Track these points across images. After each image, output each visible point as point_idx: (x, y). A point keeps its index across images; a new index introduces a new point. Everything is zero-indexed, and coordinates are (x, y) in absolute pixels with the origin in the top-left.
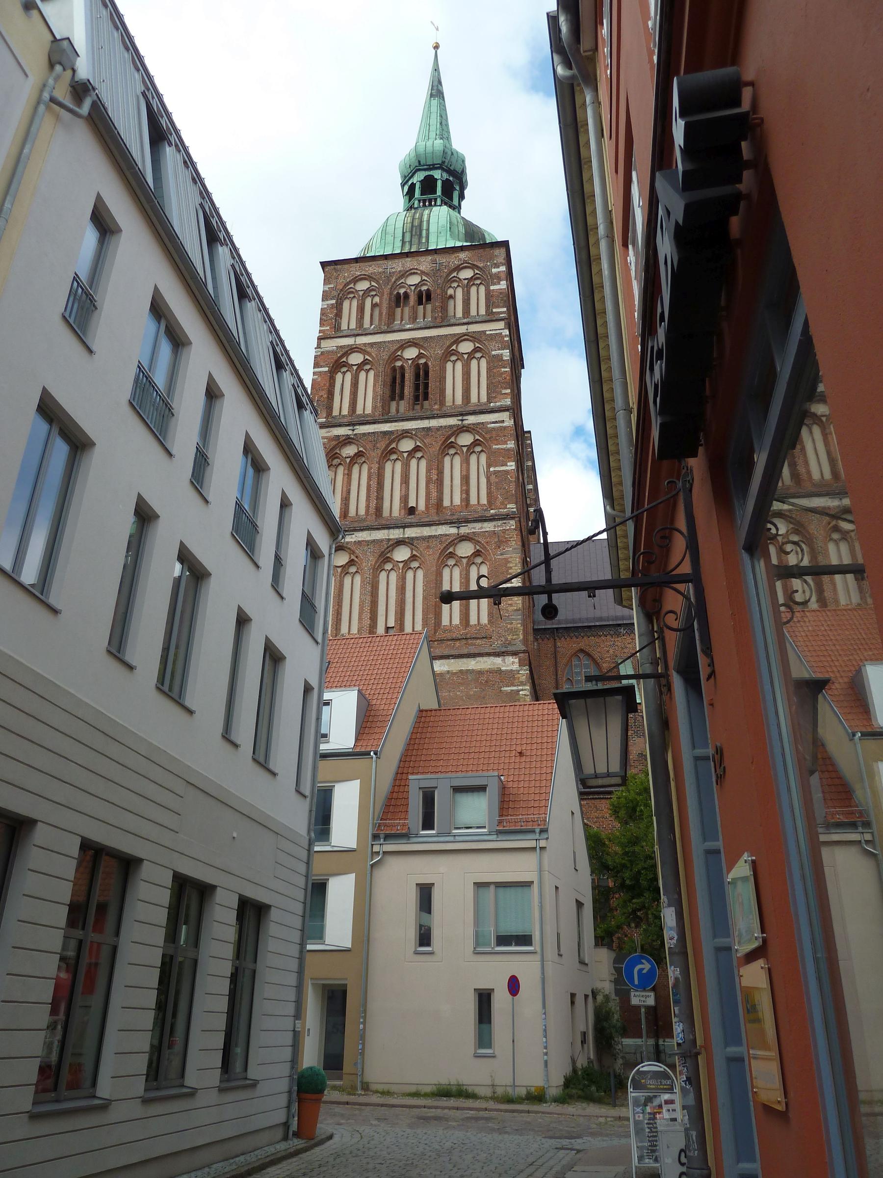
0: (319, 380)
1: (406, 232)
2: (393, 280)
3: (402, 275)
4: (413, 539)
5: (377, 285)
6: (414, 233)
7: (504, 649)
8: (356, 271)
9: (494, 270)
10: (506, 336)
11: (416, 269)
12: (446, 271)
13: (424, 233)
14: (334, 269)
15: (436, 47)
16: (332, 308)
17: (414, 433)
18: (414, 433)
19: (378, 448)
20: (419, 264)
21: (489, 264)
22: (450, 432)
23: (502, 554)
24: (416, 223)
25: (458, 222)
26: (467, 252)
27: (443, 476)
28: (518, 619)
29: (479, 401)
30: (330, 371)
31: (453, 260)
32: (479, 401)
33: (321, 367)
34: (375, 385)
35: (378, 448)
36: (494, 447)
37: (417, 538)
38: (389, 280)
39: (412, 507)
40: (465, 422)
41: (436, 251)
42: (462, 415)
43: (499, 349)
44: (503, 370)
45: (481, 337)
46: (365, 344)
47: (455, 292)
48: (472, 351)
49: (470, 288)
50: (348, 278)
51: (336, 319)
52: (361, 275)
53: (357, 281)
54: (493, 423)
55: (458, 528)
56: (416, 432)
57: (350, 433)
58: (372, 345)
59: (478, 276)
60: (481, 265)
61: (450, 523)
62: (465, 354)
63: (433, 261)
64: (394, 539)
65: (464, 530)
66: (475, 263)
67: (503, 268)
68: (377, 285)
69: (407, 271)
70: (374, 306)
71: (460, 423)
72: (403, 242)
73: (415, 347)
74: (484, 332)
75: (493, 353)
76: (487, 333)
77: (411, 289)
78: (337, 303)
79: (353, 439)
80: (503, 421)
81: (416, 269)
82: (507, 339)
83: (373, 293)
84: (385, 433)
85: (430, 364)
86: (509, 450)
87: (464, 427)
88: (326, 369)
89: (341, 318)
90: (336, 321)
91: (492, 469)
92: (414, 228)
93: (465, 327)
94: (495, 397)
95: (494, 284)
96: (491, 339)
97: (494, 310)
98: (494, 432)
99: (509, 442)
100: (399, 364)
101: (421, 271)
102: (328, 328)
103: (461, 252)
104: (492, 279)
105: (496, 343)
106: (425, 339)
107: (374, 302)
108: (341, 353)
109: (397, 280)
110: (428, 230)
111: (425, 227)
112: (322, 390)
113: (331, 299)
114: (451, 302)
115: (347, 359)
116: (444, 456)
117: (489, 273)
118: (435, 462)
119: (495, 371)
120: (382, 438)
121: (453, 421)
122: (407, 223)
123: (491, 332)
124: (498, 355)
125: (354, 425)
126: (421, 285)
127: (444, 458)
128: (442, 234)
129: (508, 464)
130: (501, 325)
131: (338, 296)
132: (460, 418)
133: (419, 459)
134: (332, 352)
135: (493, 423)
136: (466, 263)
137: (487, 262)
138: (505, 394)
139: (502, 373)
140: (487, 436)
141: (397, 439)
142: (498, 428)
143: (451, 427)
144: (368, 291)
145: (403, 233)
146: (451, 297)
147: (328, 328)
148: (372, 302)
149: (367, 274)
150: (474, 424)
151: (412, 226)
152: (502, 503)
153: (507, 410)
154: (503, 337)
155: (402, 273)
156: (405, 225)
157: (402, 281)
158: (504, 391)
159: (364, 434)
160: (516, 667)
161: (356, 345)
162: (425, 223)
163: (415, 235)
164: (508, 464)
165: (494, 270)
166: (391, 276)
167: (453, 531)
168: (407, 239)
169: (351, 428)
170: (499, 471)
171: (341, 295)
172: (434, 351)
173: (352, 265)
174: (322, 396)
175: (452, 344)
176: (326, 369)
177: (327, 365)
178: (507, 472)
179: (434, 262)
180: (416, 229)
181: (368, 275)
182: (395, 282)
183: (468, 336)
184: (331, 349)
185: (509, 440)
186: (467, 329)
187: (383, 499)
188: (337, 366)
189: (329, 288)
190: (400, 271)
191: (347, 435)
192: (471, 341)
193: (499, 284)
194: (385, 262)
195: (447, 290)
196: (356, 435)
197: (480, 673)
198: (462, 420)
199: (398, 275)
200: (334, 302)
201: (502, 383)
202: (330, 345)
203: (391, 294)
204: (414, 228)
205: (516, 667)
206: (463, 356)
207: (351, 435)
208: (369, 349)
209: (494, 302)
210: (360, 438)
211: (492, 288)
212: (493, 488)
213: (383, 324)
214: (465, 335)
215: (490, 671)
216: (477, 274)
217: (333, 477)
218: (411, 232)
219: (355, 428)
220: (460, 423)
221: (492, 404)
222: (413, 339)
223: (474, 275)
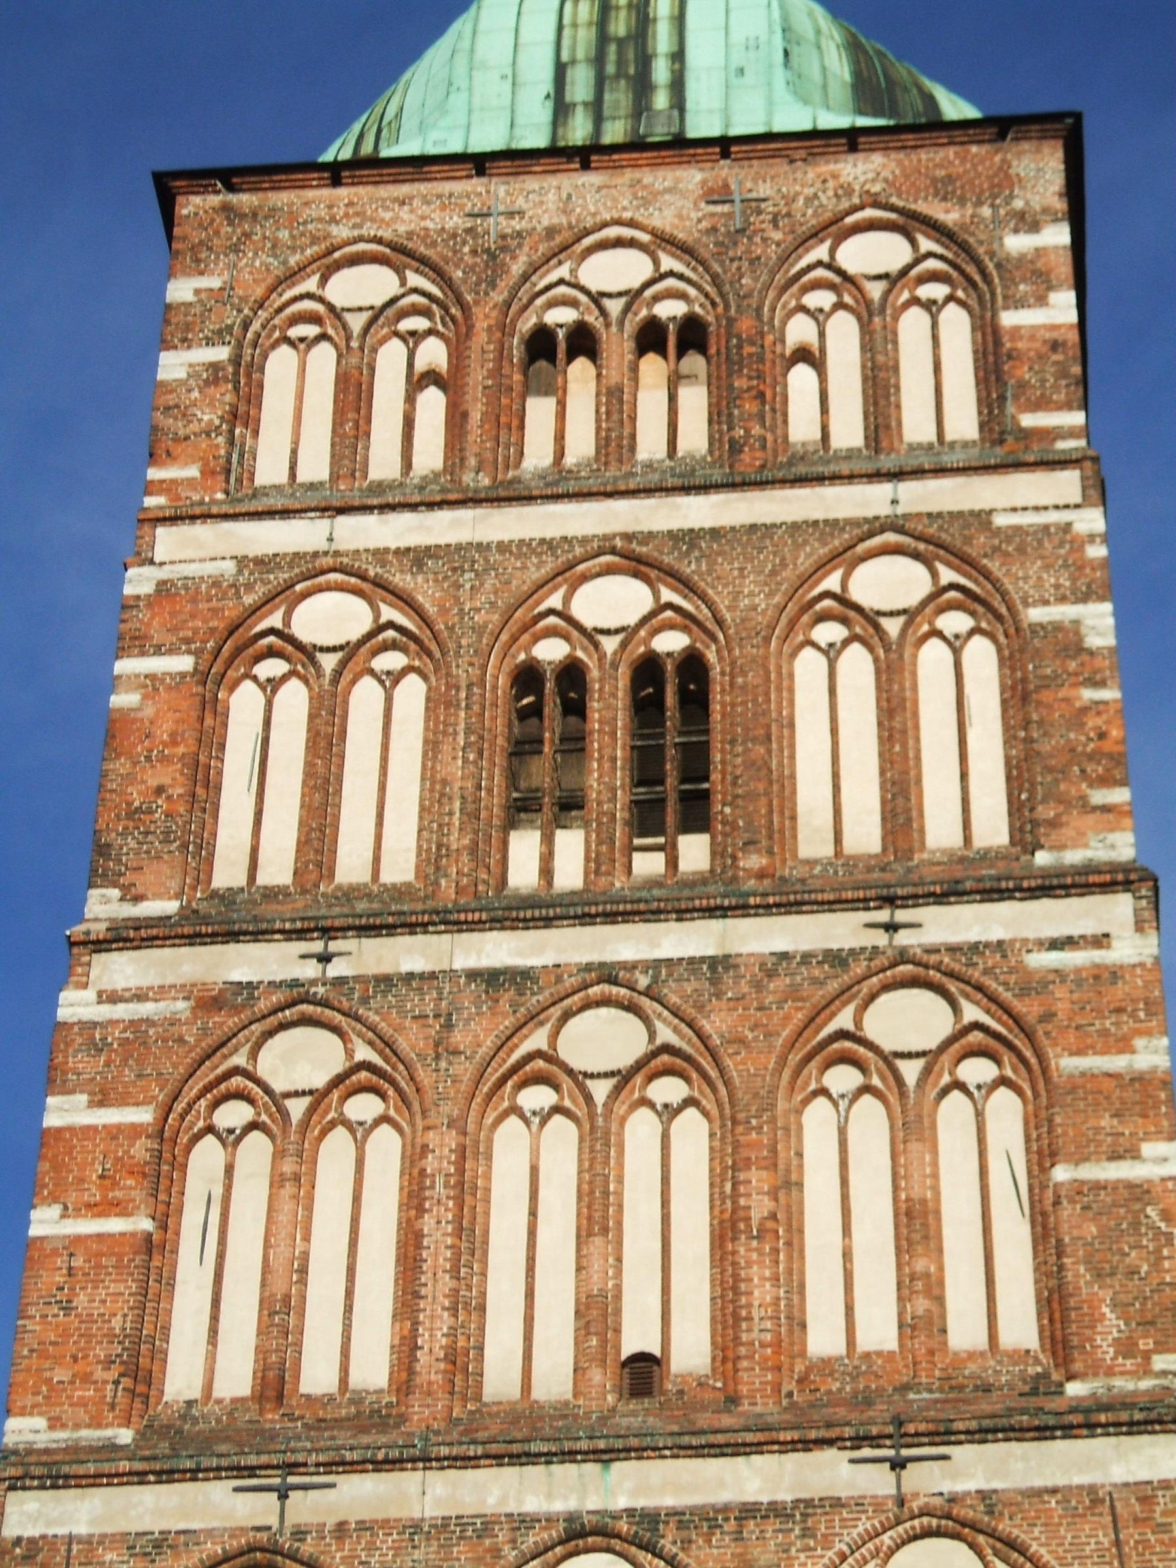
0: (149, 711)
1: (573, 62)
2: (517, 268)
3: (564, 248)
4: (650, 1519)
5: (435, 290)
6: (611, 69)
8: (333, 220)
9: (1016, 243)
10: (1092, 538)
11: (631, 224)
12: (777, 236)
14: (226, 208)
17: (643, 981)
18: (643, 981)
19: (456, 1053)
20: (646, 203)
21: (986, 211)
22: (833, 986)
24: (620, 26)
25: (818, 32)
26: (877, 159)
27: (801, 1203)
29: (967, 839)
30: (201, 676)
31: (809, 191)
32: (967, 839)
33: (158, 651)
34: (432, 747)
35: (456, 1053)
36: (1068, 1064)
39: (642, 1358)
40: (903, 938)
41: (724, 145)
42: (890, 901)
43: (1062, 599)
44: (1089, 694)
45: (968, 540)
46: (380, 555)
47: (822, 335)
48: (924, 603)
49: (896, 319)
50: (293, 249)
51: (231, 432)
52: (356, 240)
53: (338, 266)
54: (1056, 944)
55: (898, 1465)
56: (655, 979)
57: (311, 970)
58: (417, 558)
59: (932, 264)
60: (950, 216)
62: (892, 614)
63: (711, 191)
64: (550, 1520)
66: (922, 207)
67: (1058, 236)
68: (435, 290)
69: (588, 233)
70: (417, 382)
71: (880, 939)
72: (561, 109)
73: (636, 575)
74: (982, 518)
75: (1036, 614)
76: (1000, 520)
77: (603, 312)
78: (236, 360)
79: (324, 1003)
80: (1101, 941)
81: (631, 224)
82: (1097, 551)
83: (419, 323)
85: (711, 656)
87: (903, 956)
88: (184, 663)
89: (256, 433)
90: (231, 442)
91: (1061, 1173)
92: (612, 49)
93: (885, 490)
94: (1054, 824)
95: (1019, 304)
96: (1021, 550)
97: (1028, 420)
98: (1060, 992)
99: (1139, 1043)
100: (550, 651)
101: (653, 232)
102: (193, 472)
103: (851, 158)
104: (1009, 281)
105: (1047, 567)
106: (688, 539)
107: (420, 365)
108: (261, 590)
109: (535, 268)
110: (678, 56)
111: (662, 40)
112: (164, 759)
113: (209, 342)
114: (802, 378)
115: (287, 620)
116: (806, 1102)
117: (992, 254)
118: (759, 1128)
119: (1046, 696)
120: (477, 1003)
122: (575, 25)
124: (1057, 627)
125: (328, 933)
126: (657, 298)
127: (799, 1112)
128: (749, 78)
129: (1147, 1149)
131: (246, 325)
132: (883, 916)
133: (669, 1112)
135: (1056, 944)
136: (876, 205)
137: (979, 203)
138: (1106, 809)
139: (1085, 710)
140: (1029, 1009)
141: (556, 1012)
142: (1078, 970)
143: (837, 959)
144: (390, 312)
145: (561, 71)
146: (803, 355)
147: (193, 472)
148: (410, 364)
149: (386, 234)
150: (953, 949)
151: (603, 38)
152: (1126, 1347)
153: (1127, 885)
154: (1079, 544)
155: (558, 239)
156: (567, 32)
157: (563, 271)
158: (1099, 796)
159: (385, 981)
161: (337, 554)
163: (618, 76)
164: (1147, 1149)
165: (1016, 243)
166: (504, 249)
169: (317, 946)
170: (1098, 1186)
171: (256, 326)
172: (736, 595)
173: (310, 194)
174: (160, 790)
175: (823, 567)
176: (184, 663)
177: (187, 641)
178: (1139, 1192)
179: (718, 195)
180: (620, 53)
181: (389, 245)
182: (525, 277)
183: (901, 530)
184: (210, 569)
185: (1139, 1033)
186: (894, 502)
187: (482, 1308)
188: (238, 651)
189: (197, 292)
190: (551, 232)
191: (295, 983)
192: (916, 556)
193: (1042, 301)
194: (477, 184)
195: (784, 323)
196: (340, 981)
198: (891, 927)
199: (542, 249)
200: (221, 353)
201: (1092, 757)
203: (504, 328)
204: (612, 49)
206: (877, 627)
207: (313, 982)
208: (401, 579)
209: (1022, 385)
210: (365, 1000)
211: (1009, 319)
212: (1078, 1273)
213: (472, 462)
214: (876, 526)
216: (930, 254)
217: (218, 1191)
218: (599, 60)
219: (334, 946)
220: (880, 939)
221: (1042, 858)
222: (628, 537)
223: (917, 261)
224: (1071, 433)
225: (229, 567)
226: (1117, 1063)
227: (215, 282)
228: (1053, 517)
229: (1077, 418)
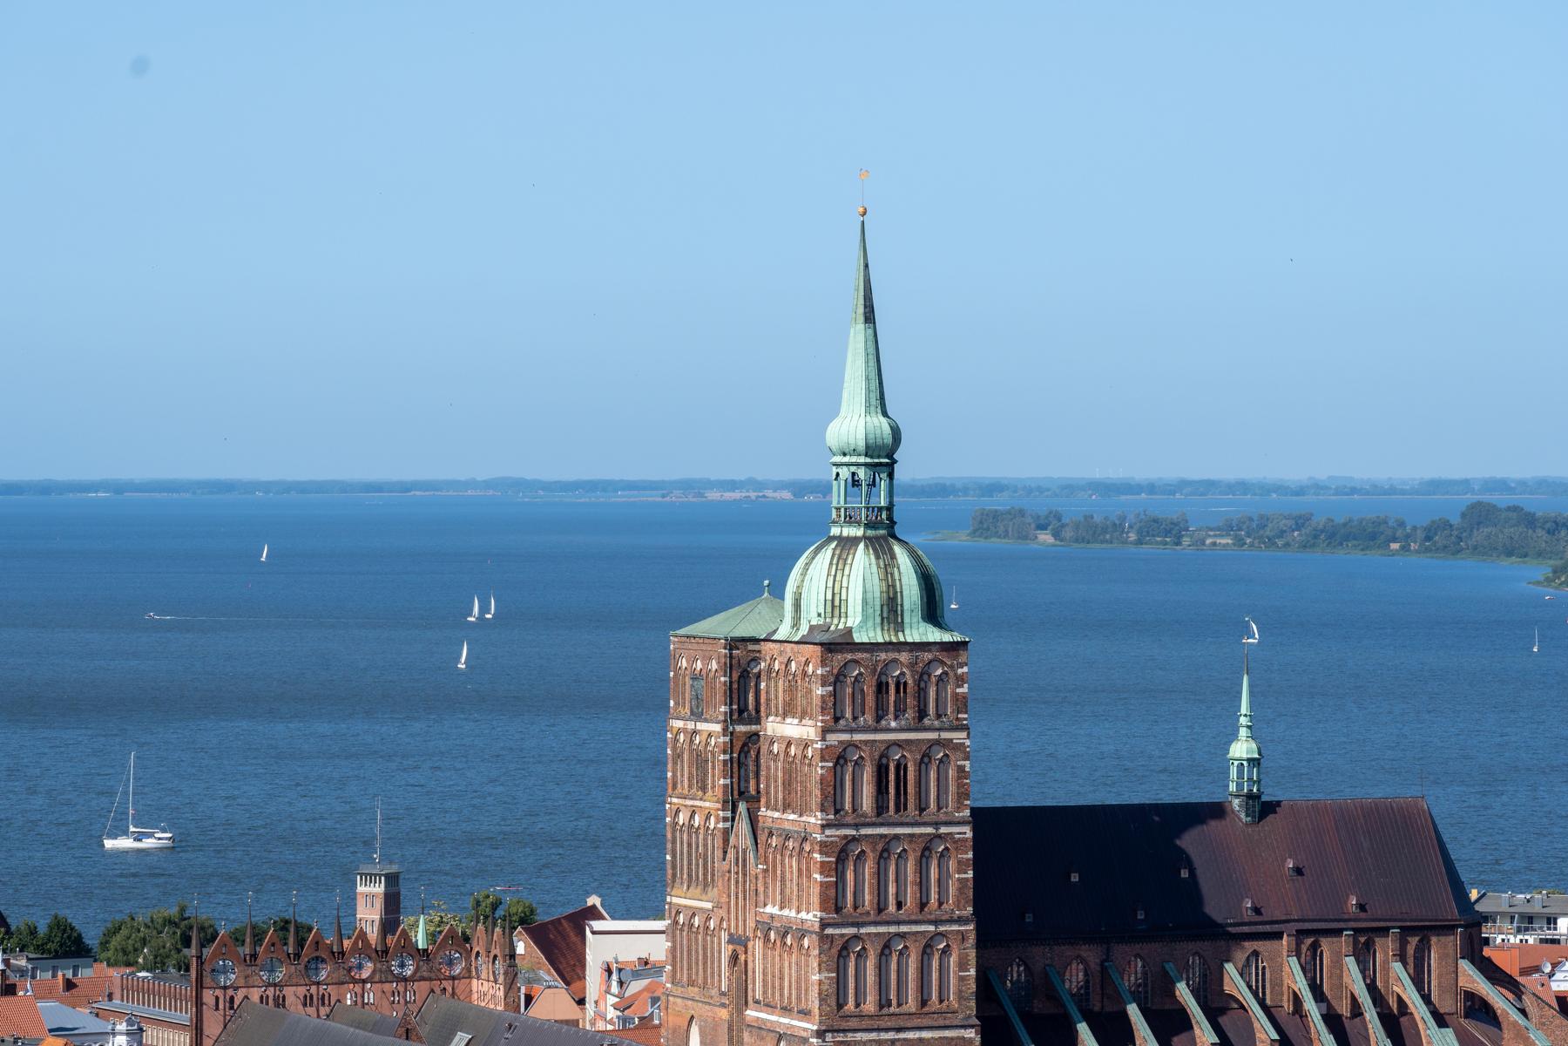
7: (966, 1023)
10: (968, 746)
13: (899, 608)
15: (864, 213)
16: (830, 696)
23: (964, 949)
24: (891, 595)
28: (972, 999)
37: (909, 933)
38: (875, 670)
61: (930, 922)
65: (942, 929)
71: (934, 831)
74: (952, 740)
76: (955, 741)
80: (965, 833)
84: (882, 836)
86: (968, 860)
110: (902, 605)
121: (930, 830)
123: (958, 741)
130: (964, 735)
134: (835, 746)
145: (882, 606)
159: (866, 836)
160: (973, 1035)
162: (899, 594)
167: (932, 928)
168: (885, 615)
176: (831, 764)
197: (952, 1039)
200: (831, 688)
202: (834, 738)
205: (973, 1035)
215: (958, 1038)
224: (965, 719)
225: (837, 743)
226: (965, 856)
227: (828, 669)
228: (962, 741)
229: (966, 716)
